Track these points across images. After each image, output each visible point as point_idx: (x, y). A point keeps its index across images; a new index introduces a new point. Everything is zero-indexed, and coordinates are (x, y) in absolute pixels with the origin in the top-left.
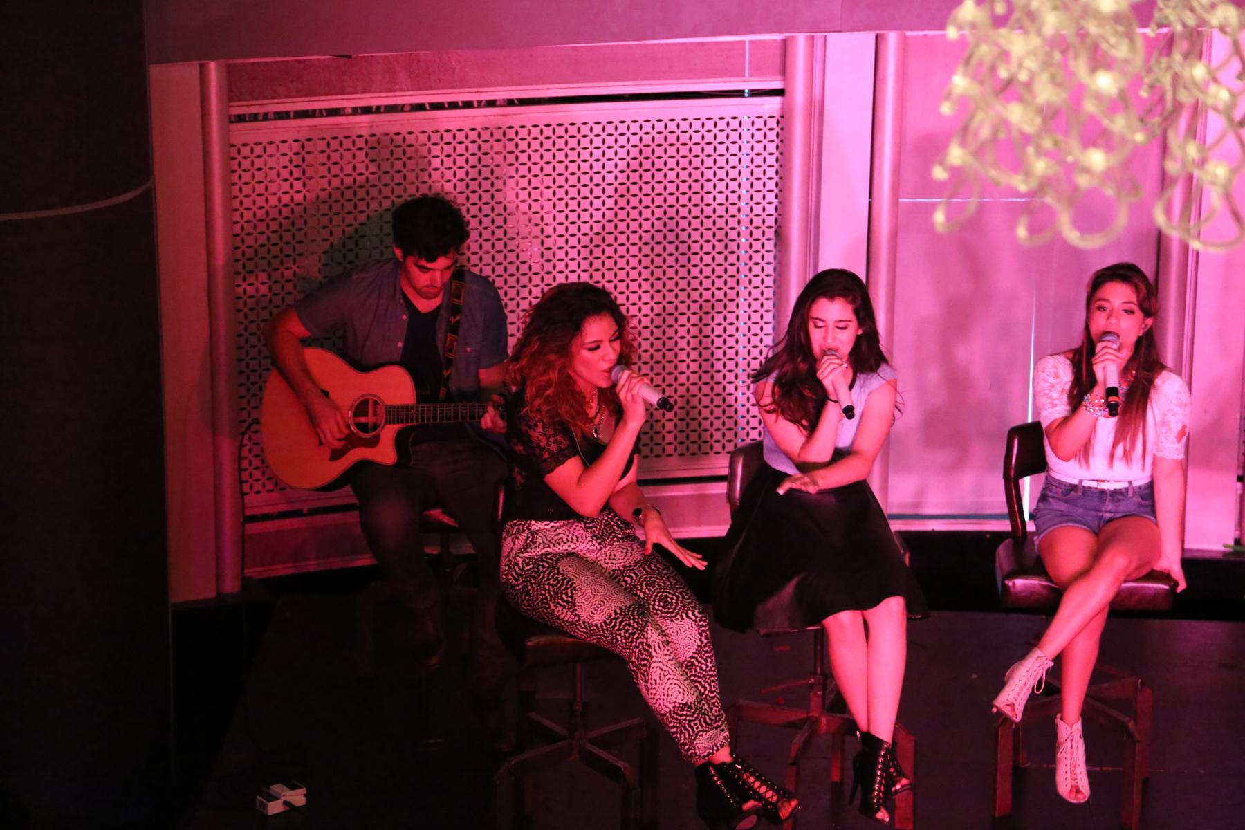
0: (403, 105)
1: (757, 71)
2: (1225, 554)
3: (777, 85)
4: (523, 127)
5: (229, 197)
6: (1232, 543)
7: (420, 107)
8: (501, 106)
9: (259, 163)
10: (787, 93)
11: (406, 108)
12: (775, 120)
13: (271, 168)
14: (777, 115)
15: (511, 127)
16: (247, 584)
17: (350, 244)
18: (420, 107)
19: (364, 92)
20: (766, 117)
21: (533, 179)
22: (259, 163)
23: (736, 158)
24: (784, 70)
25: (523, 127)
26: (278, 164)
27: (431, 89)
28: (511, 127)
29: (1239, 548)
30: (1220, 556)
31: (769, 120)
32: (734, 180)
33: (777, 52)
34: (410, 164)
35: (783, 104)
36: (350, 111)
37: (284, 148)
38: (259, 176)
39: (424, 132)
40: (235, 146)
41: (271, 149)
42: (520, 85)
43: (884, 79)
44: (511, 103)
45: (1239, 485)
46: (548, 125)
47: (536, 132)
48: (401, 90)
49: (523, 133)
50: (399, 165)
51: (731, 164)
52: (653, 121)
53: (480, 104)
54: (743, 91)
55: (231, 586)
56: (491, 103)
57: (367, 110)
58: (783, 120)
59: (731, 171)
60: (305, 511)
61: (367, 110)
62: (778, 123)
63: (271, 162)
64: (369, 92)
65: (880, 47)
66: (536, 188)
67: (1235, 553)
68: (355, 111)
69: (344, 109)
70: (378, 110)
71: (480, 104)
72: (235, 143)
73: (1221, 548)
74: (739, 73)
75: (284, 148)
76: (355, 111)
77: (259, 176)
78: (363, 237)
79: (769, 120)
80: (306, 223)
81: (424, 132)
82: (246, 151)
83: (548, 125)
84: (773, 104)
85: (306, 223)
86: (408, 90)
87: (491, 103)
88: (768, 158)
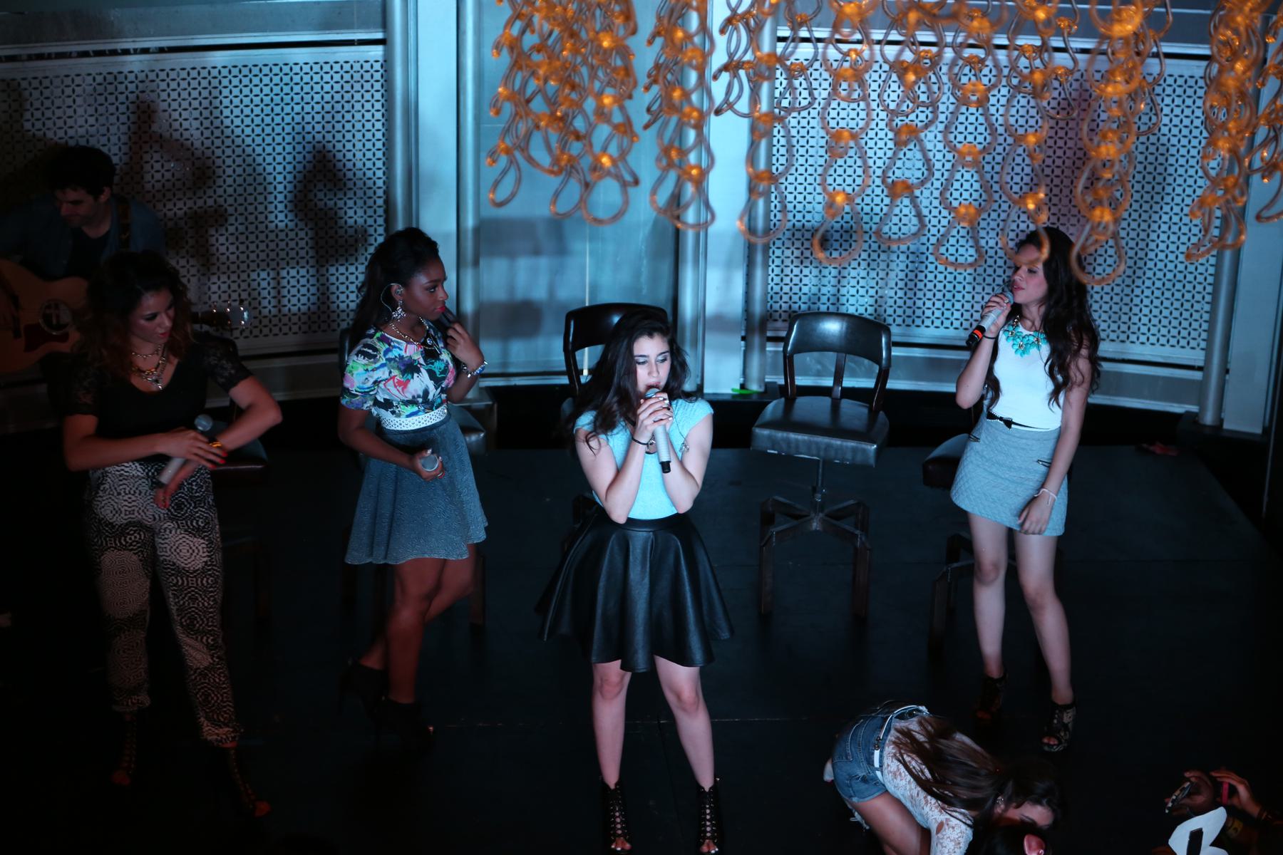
0: (71, 53)
1: (365, 25)
2: (734, 396)
3: (379, 36)
4: (173, 70)
6: (738, 387)
7: (85, 54)
8: (153, 53)
10: (388, 42)
11: (74, 55)
12: (379, 64)
14: (381, 59)
15: (162, 70)
18: (85, 54)
19: (36, 42)
20: (372, 61)
21: (183, 113)
23: (350, 95)
24: (385, 24)
25: (173, 70)
27: (93, 39)
28: (162, 70)
29: (744, 392)
30: (729, 398)
31: (375, 64)
32: (348, 112)
33: (379, 10)
35: (385, 51)
36: (25, 57)
39: (89, 75)
42: (168, 35)
43: (465, 32)
44: (161, 50)
45: (743, 343)
46: (194, 68)
47: (184, 74)
48: (68, 40)
49: (173, 75)
50: (69, 102)
51: (346, 99)
52: (281, 65)
53: (136, 52)
54: (353, 41)
56: (145, 51)
57: (40, 57)
58: (387, 63)
59: (346, 105)
61: (40, 57)
62: (382, 66)
64: (42, 42)
65: (461, 9)
66: (186, 120)
67: (741, 395)
68: (30, 58)
69: (20, 56)
70: (49, 57)
71: (136, 52)
73: (730, 391)
74: (349, 26)
76: (30, 58)
79: (375, 64)
81: (89, 75)
83: (194, 68)
84: (377, 52)
86: (75, 40)
87: (145, 51)
88: (375, 94)
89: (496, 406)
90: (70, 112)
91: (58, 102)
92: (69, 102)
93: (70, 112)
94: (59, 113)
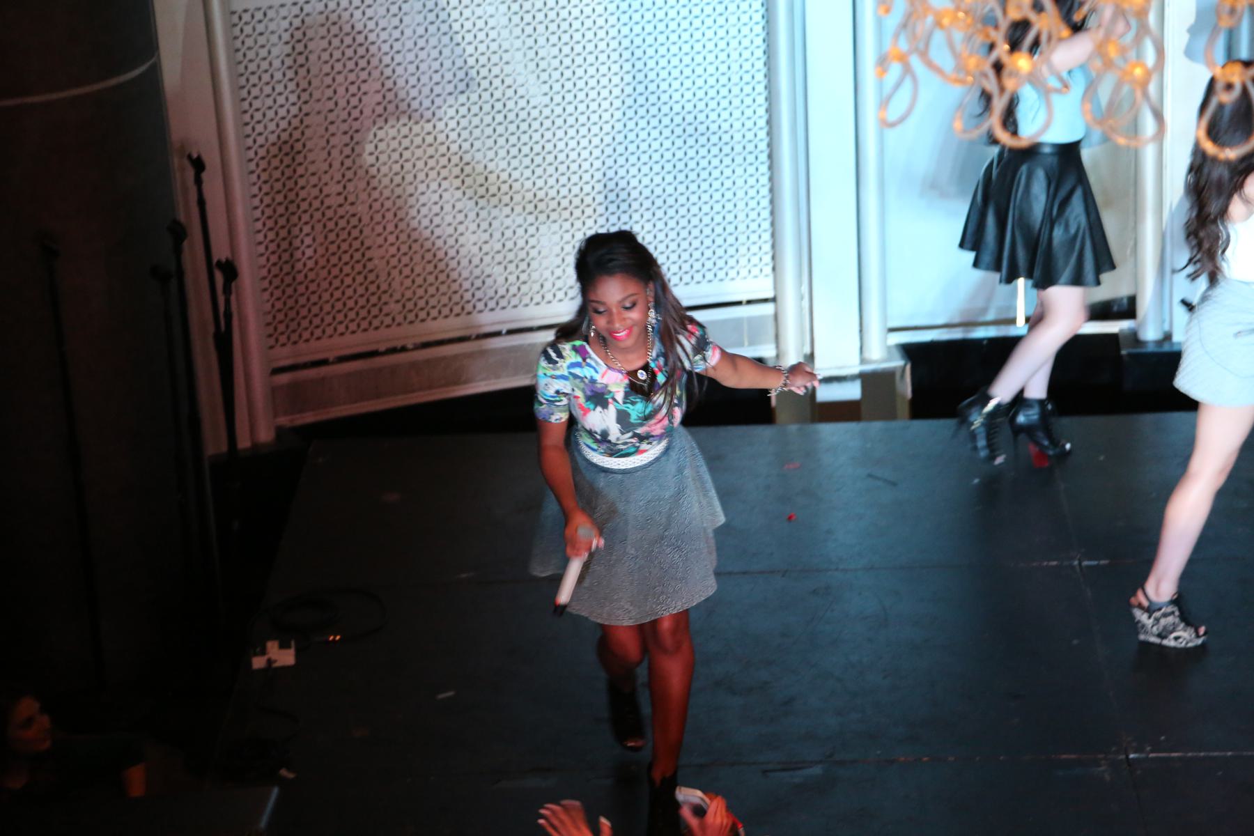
5: (234, 64)
9: (260, 28)
13: (272, 32)
16: (280, 432)
17: (354, 101)
22: (260, 28)
26: (279, 27)
34: (407, 20)
37: (283, 12)
38: (262, 40)
40: (233, 13)
41: (271, 14)
55: (265, 435)
60: (331, 360)
63: (272, 26)
72: (234, 9)
75: (283, 12)
77: (262, 40)
78: (365, 93)
80: (310, 83)
82: (246, 17)
85: (310, 83)
89: (908, 367)
90: (396, 34)
91: (382, 24)
92: (396, 21)
93: (396, 34)
94: (384, 35)
